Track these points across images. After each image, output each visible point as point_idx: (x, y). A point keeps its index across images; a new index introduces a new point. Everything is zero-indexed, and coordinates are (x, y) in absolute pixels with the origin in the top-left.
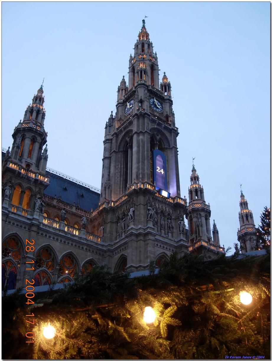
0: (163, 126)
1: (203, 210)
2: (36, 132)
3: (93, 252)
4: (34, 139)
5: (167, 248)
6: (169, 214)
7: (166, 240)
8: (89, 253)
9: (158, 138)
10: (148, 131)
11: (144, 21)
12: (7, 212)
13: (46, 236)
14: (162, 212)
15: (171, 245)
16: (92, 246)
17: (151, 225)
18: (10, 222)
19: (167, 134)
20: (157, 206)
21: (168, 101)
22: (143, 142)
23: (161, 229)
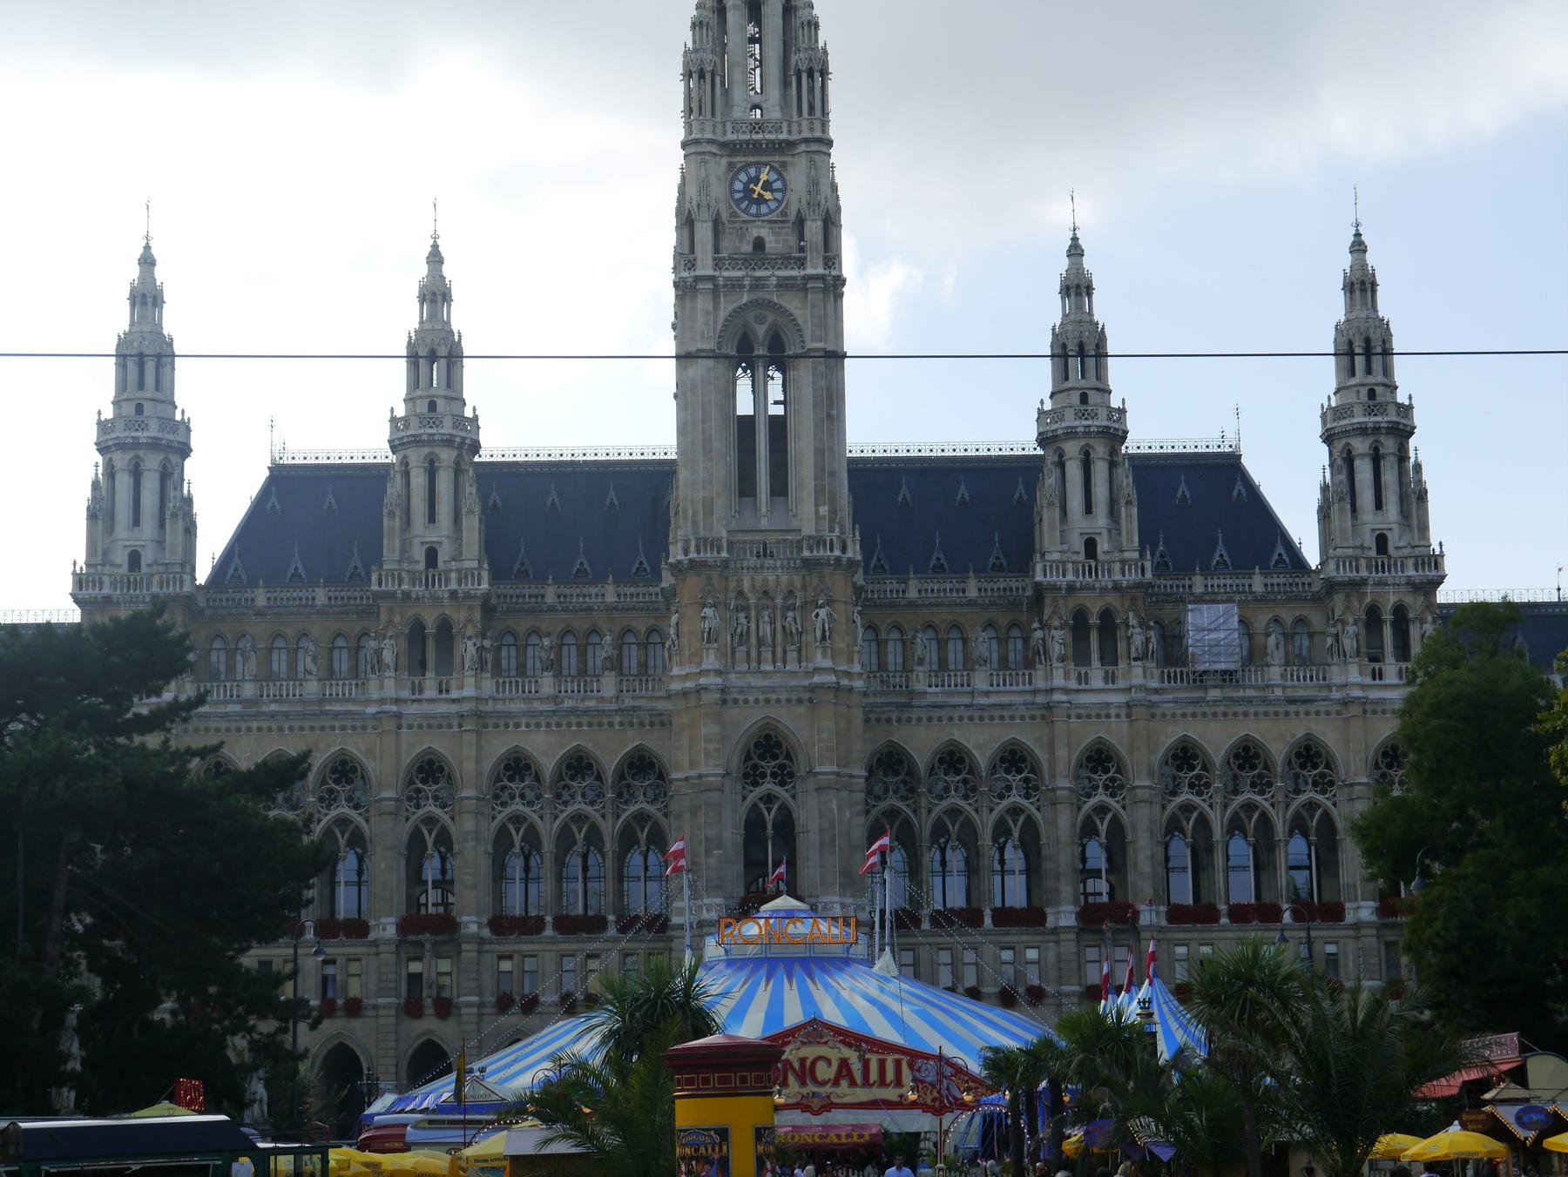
0: (773, 281)
1: (1071, 434)
2: (431, 441)
3: (642, 724)
4: (432, 462)
5: (778, 701)
6: (791, 592)
7: (777, 680)
8: (630, 733)
9: (761, 331)
10: (706, 346)
12: (394, 708)
13: (507, 726)
14: (765, 592)
15: (792, 689)
16: (634, 709)
17: (711, 661)
18: (410, 727)
19: (791, 303)
20: (746, 585)
21: (803, 148)
23: (759, 653)
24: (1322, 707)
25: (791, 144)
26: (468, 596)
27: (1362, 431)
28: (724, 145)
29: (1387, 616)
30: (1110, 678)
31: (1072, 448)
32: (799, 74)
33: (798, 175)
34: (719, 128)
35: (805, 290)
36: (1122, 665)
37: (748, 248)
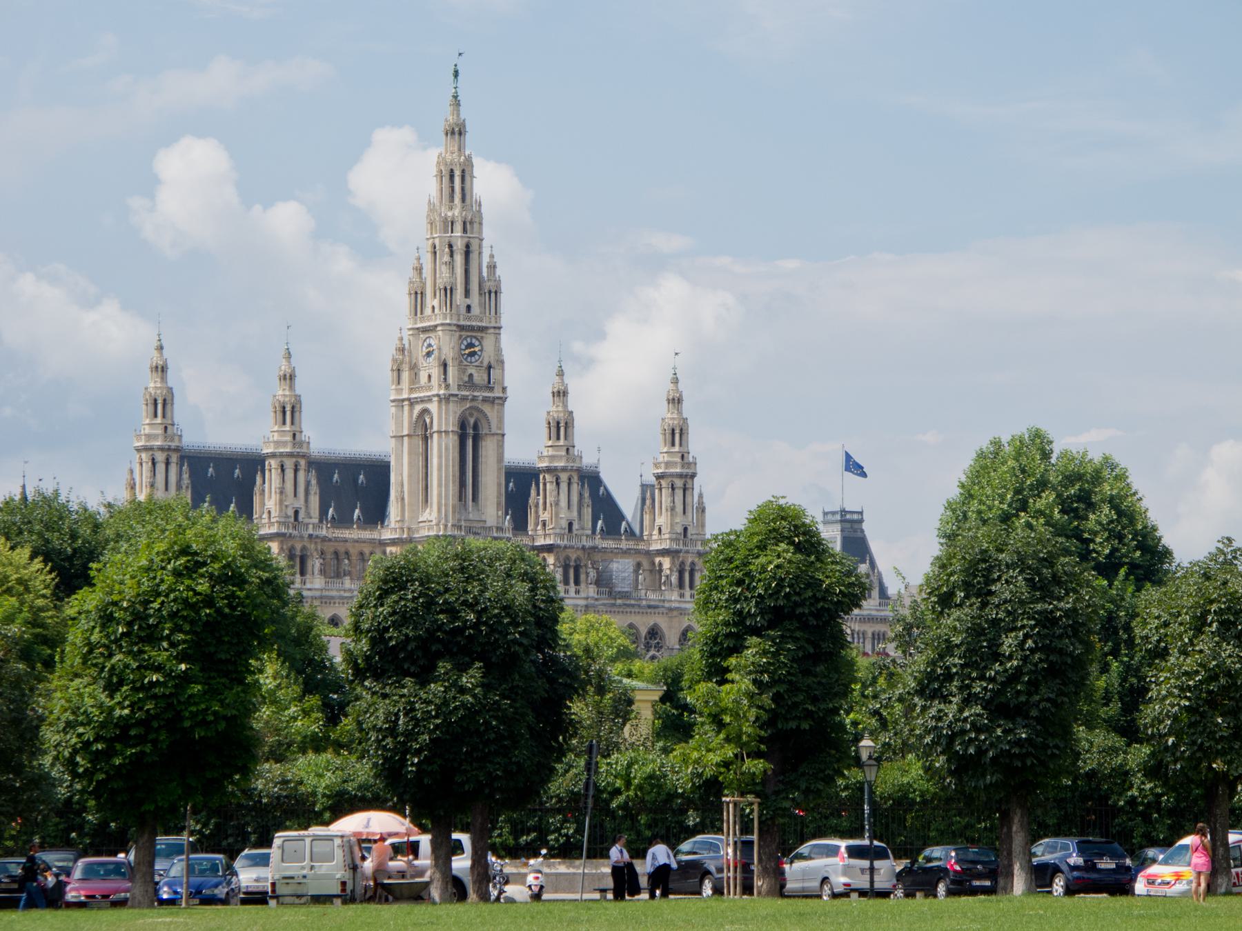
9: (472, 421)
11: (456, 74)
19: (486, 408)
21: (492, 331)
22: (447, 449)
24: (661, 610)
25: (487, 328)
26: (317, 537)
27: (681, 476)
28: (458, 326)
29: (688, 568)
30: (577, 592)
31: (564, 477)
32: (490, 292)
33: (488, 342)
34: (455, 317)
35: (493, 402)
36: (583, 586)
37: (466, 379)
